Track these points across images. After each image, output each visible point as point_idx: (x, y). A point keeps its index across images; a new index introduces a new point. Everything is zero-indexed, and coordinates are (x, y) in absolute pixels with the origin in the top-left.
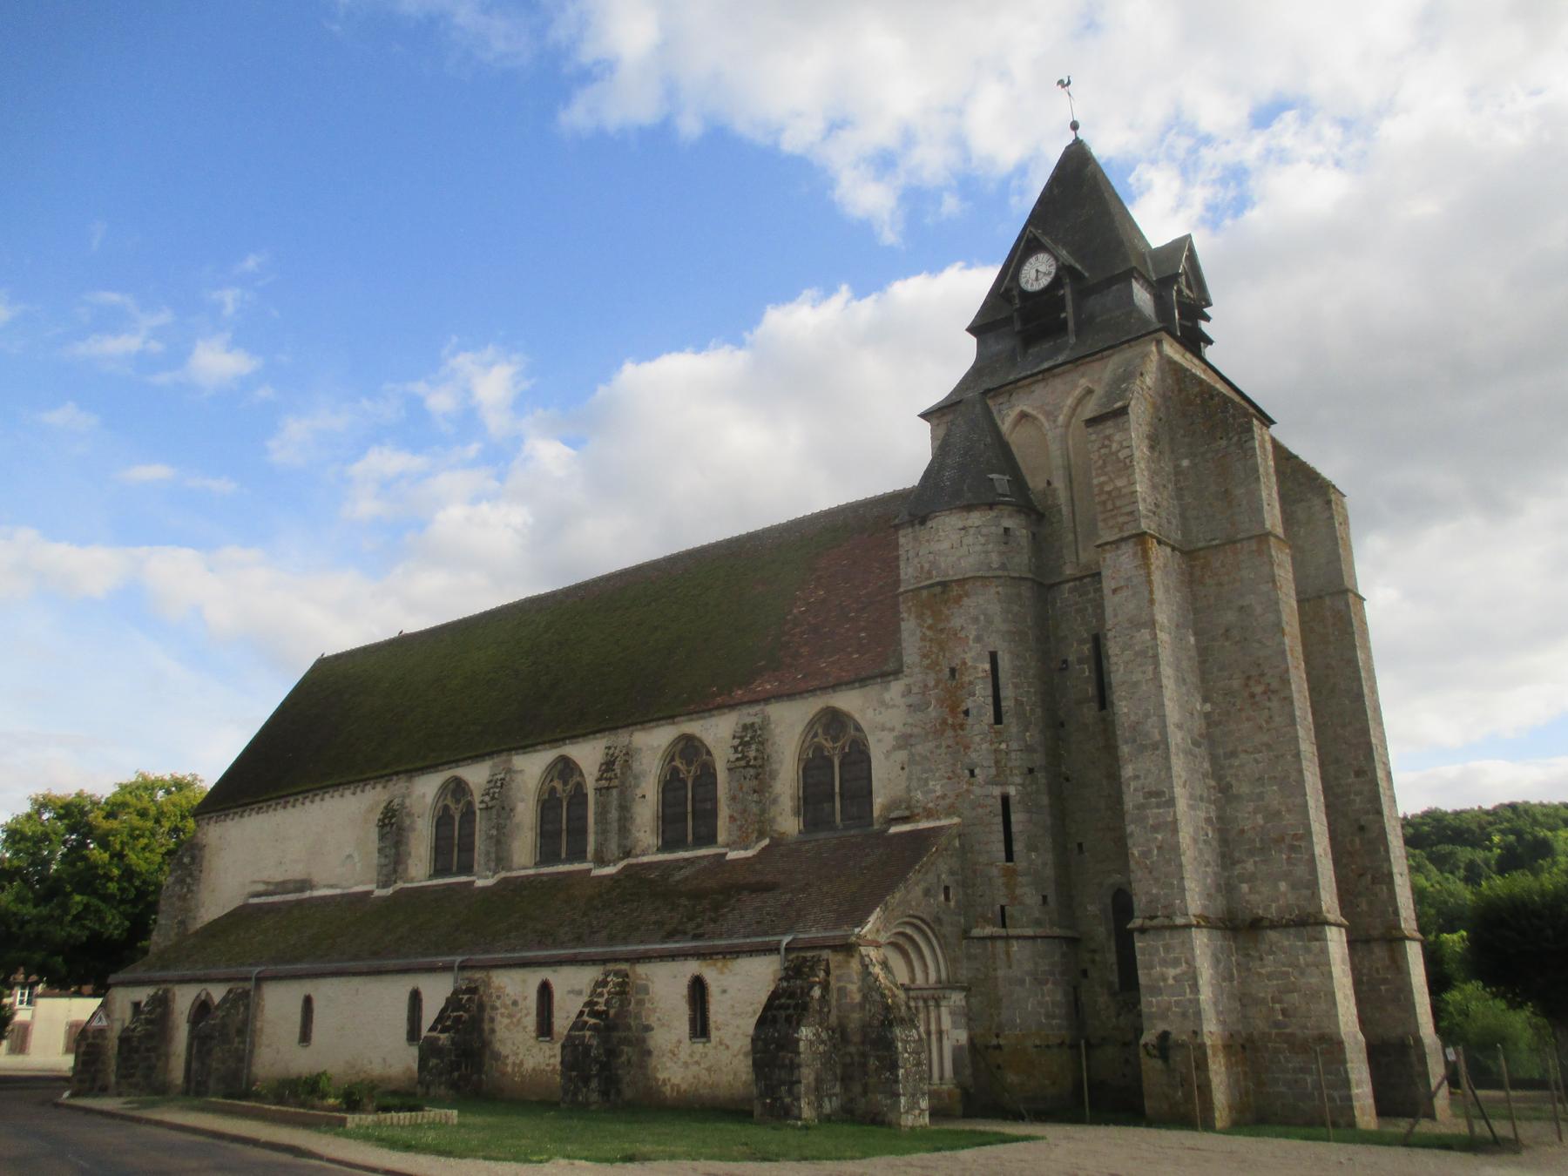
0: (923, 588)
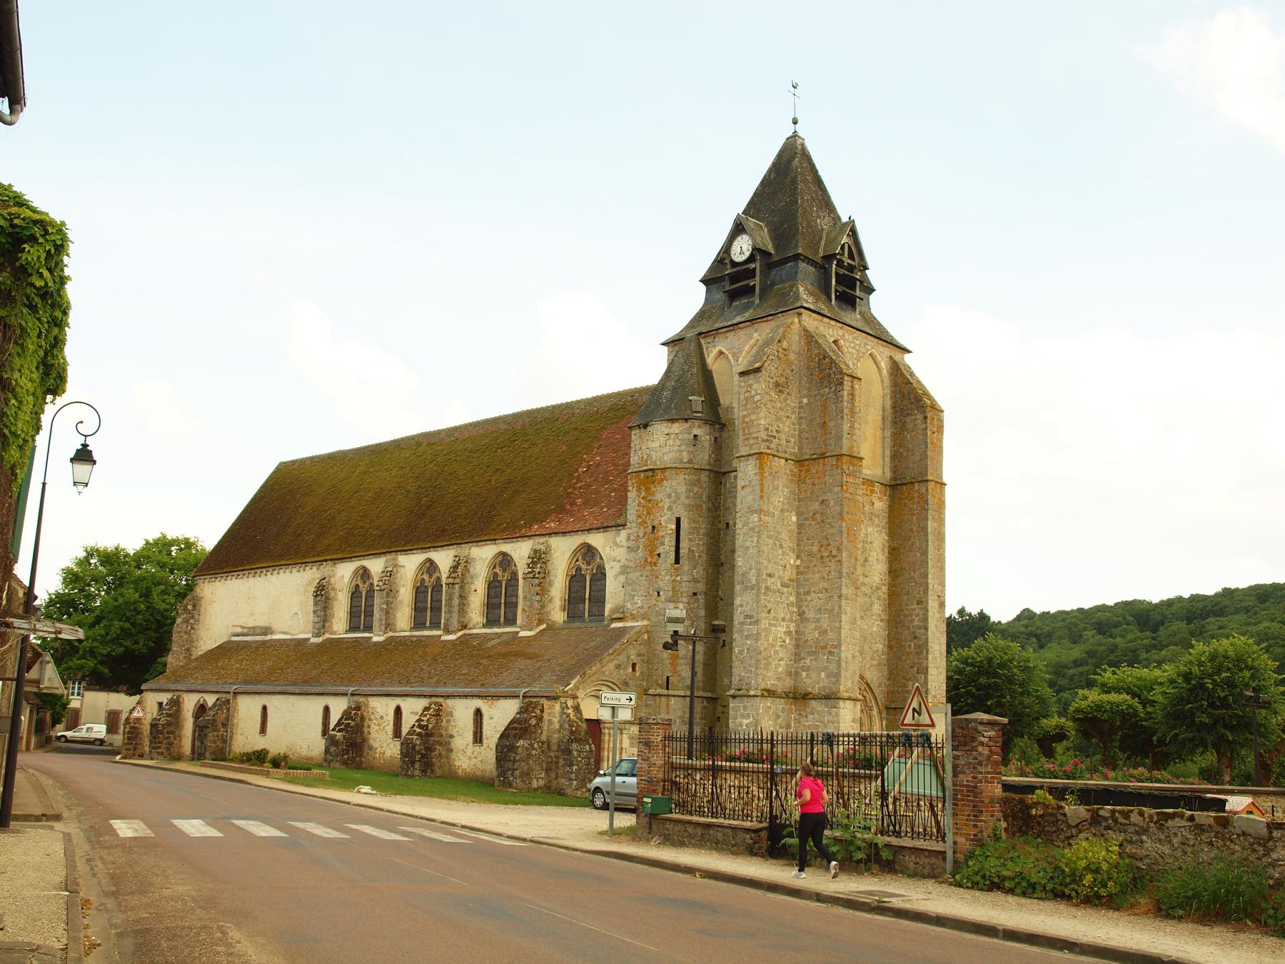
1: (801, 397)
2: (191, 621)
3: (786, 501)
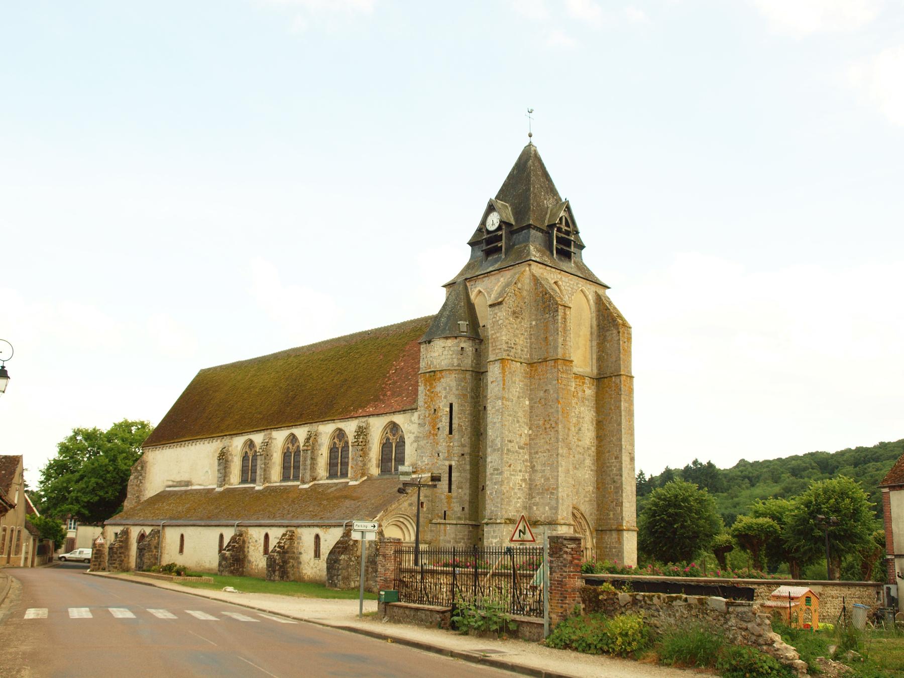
0: (427, 372)
1: (531, 321)
2: (140, 478)
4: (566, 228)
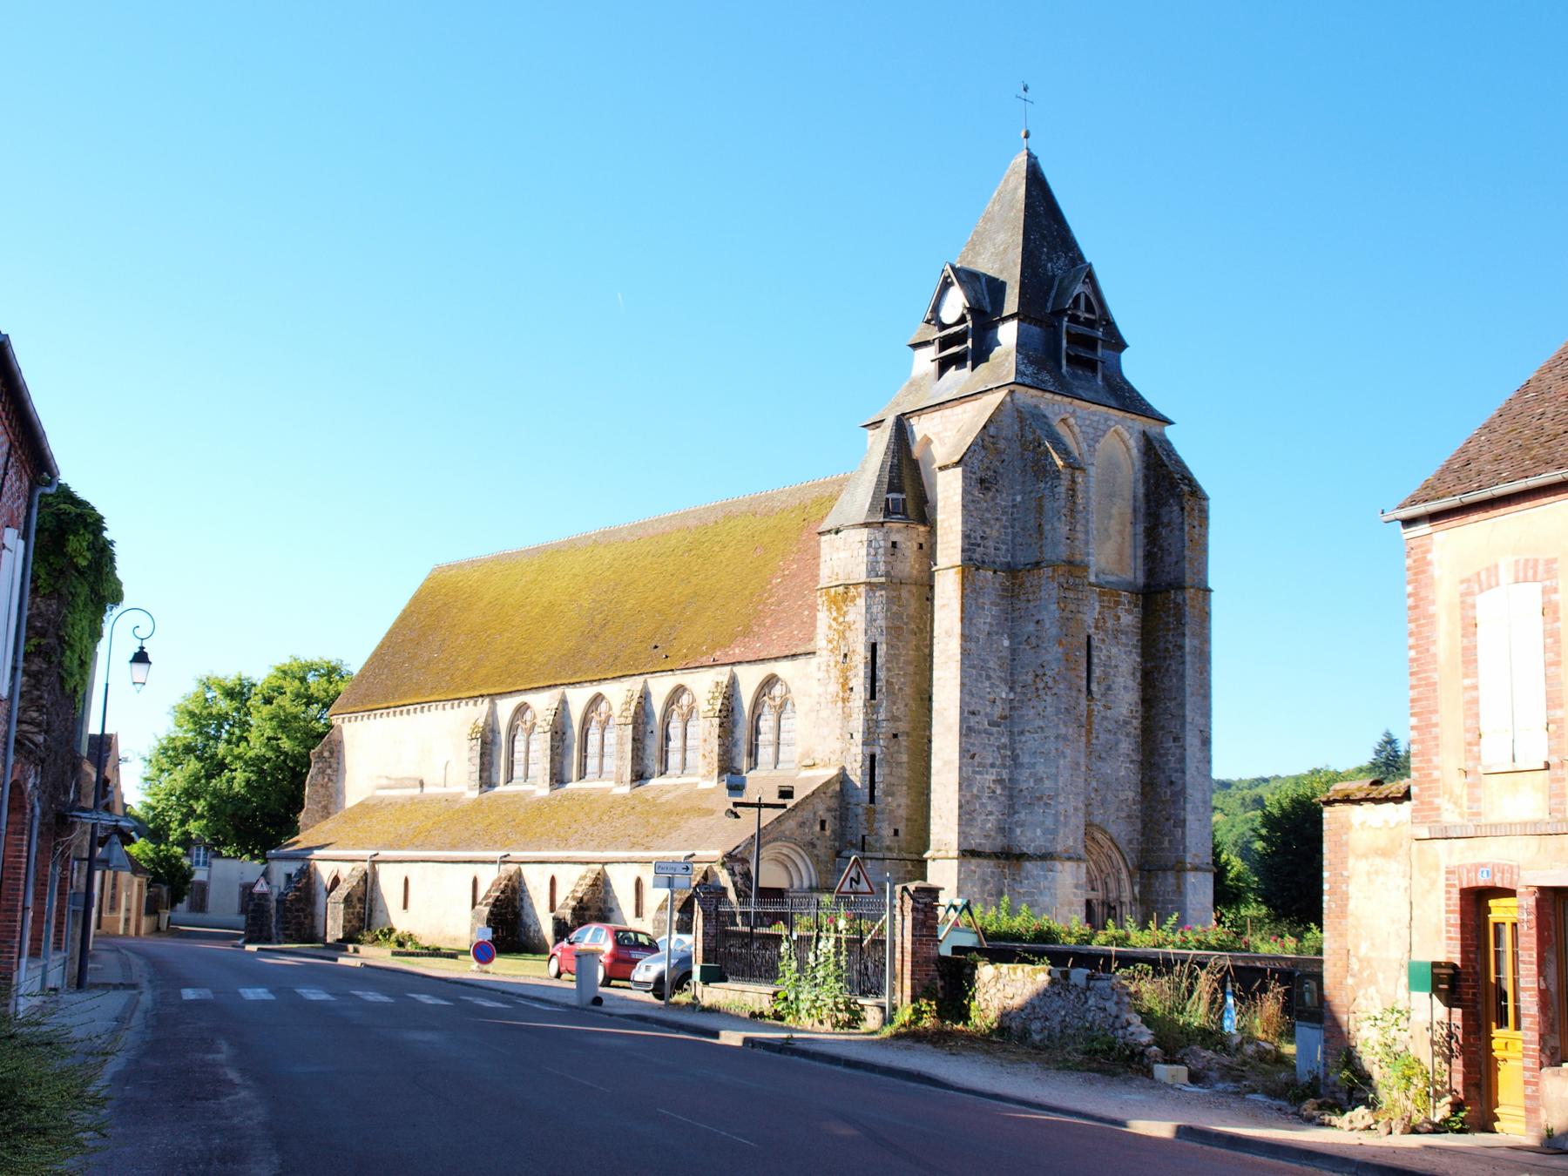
1: (1014, 494)
2: (329, 771)
3: (994, 623)
4: (1087, 316)
